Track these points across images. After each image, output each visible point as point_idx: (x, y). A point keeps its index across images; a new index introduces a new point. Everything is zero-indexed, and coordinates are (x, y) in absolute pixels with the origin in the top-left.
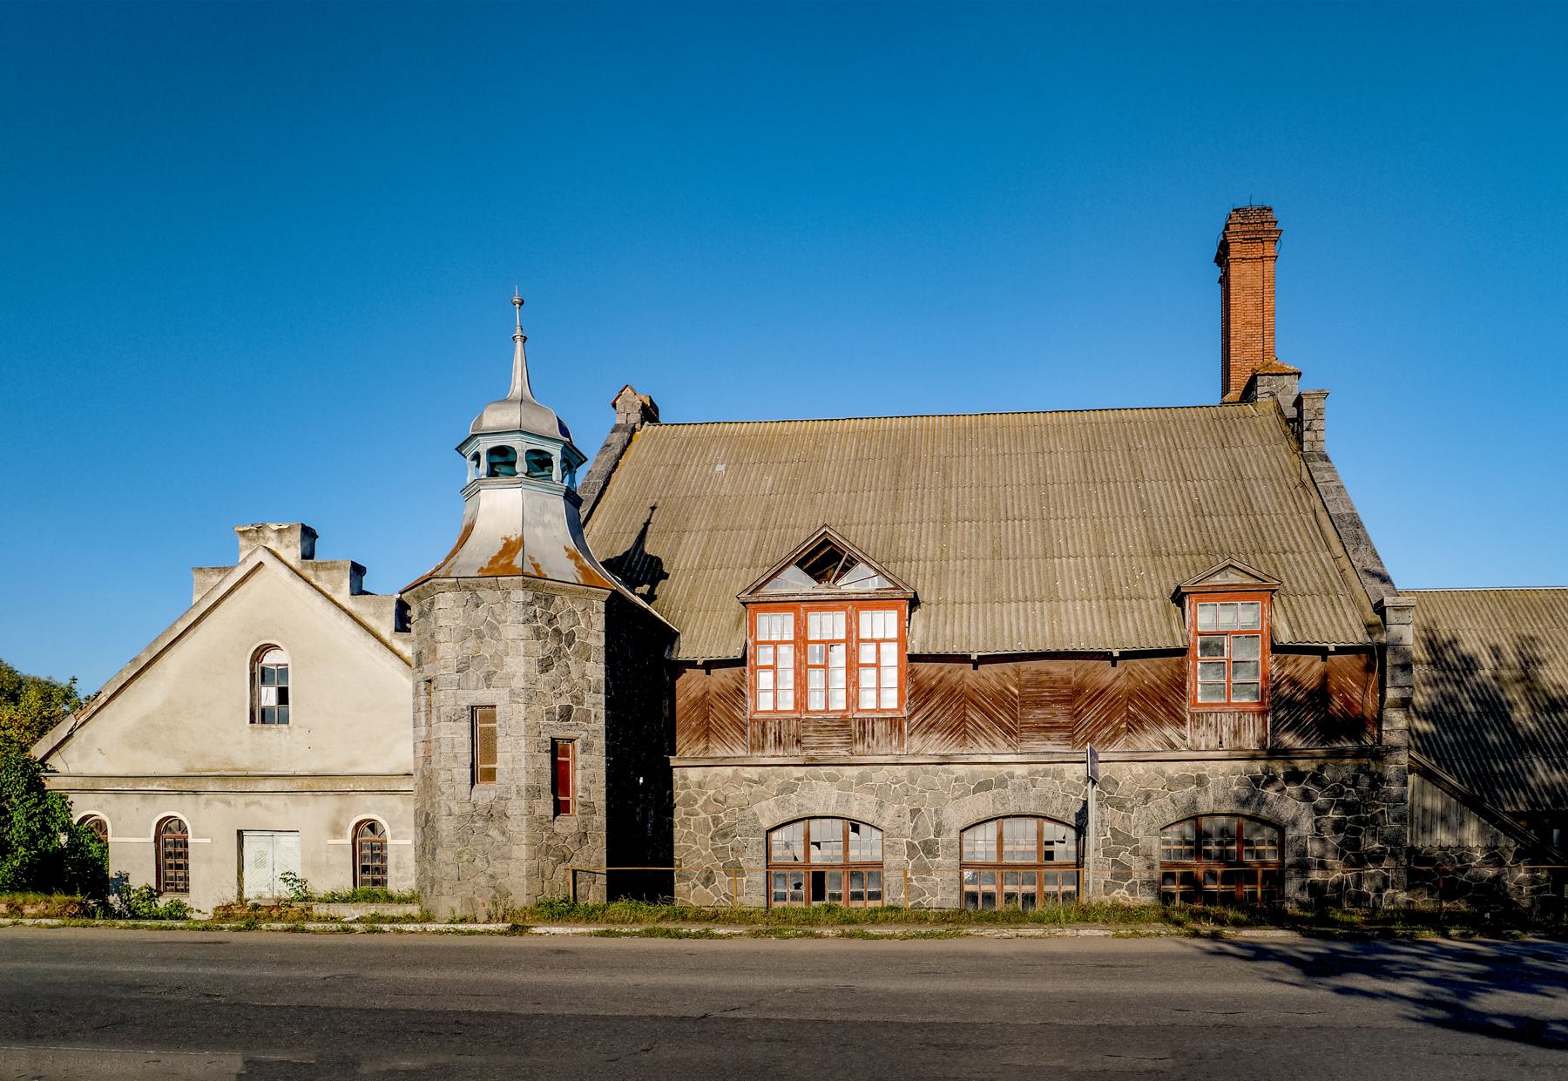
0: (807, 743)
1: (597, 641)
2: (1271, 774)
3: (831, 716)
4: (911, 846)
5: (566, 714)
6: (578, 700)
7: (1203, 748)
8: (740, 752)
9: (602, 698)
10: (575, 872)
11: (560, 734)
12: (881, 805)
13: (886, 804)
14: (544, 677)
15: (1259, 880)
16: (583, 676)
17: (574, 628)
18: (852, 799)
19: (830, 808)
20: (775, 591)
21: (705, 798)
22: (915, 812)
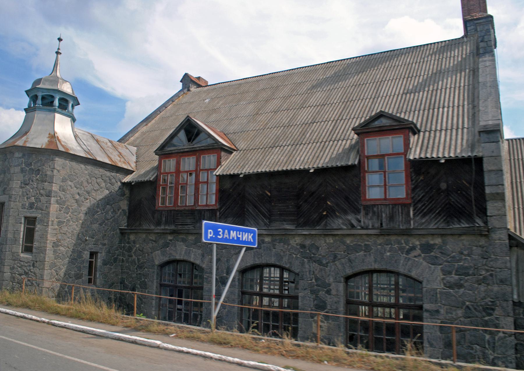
0: (177, 222)
2: (411, 245)
3: (187, 208)
5: (31, 206)
6: (38, 200)
7: (370, 227)
8: (153, 227)
11: (28, 215)
12: (203, 256)
13: (205, 255)
15: (271, 315)
17: (40, 168)
18: (191, 252)
19: (182, 256)
20: (169, 149)
21: (135, 248)
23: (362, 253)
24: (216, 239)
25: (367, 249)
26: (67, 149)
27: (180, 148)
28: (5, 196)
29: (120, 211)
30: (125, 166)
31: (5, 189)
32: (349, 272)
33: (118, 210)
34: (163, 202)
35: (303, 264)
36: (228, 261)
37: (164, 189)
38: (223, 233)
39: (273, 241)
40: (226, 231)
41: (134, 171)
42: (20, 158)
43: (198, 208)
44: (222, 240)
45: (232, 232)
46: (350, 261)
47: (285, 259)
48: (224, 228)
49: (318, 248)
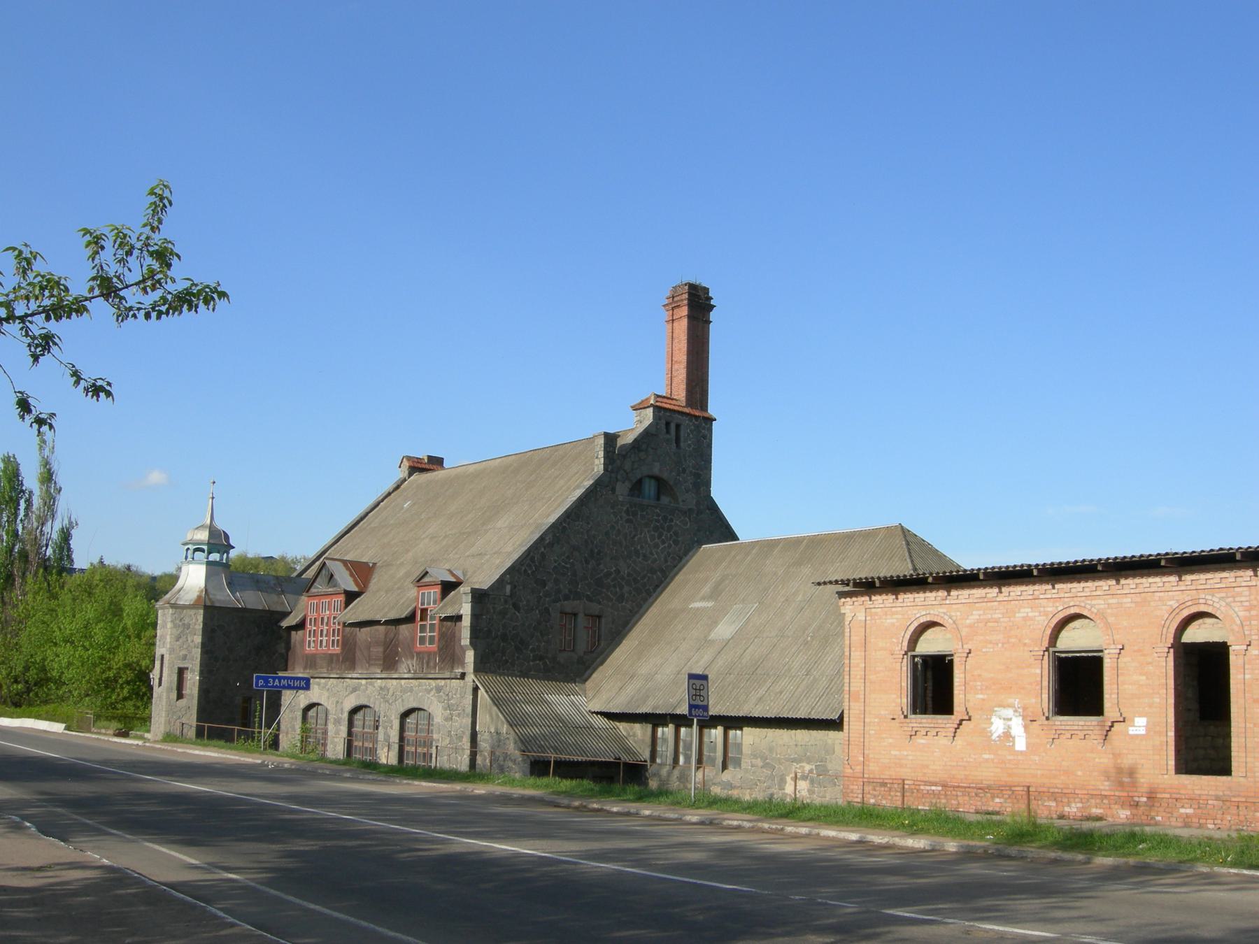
1: (199, 626)
4: (335, 719)
5: (185, 657)
9: (199, 650)
10: (183, 724)
11: (182, 666)
14: (178, 643)
16: (193, 641)
22: (337, 702)
23: (409, 694)
24: (267, 686)
25: (411, 690)
26: (213, 602)
27: (320, 590)
28: (164, 649)
29: (277, 655)
30: (279, 609)
31: (164, 642)
32: (402, 710)
33: (274, 654)
34: (309, 646)
35: (380, 704)
36: (342, 703)
37: (310, 631)
38: (274, 682)
39: (367, 683)
40: (277, 680)
41: (291, 612)
42: (175, 614)
43: (330, 652)
44: (273, 686)
45: (282, 681)
46: (403, 700)
47: (371, 700)
48: (274, 679)
49: (388, 690)
